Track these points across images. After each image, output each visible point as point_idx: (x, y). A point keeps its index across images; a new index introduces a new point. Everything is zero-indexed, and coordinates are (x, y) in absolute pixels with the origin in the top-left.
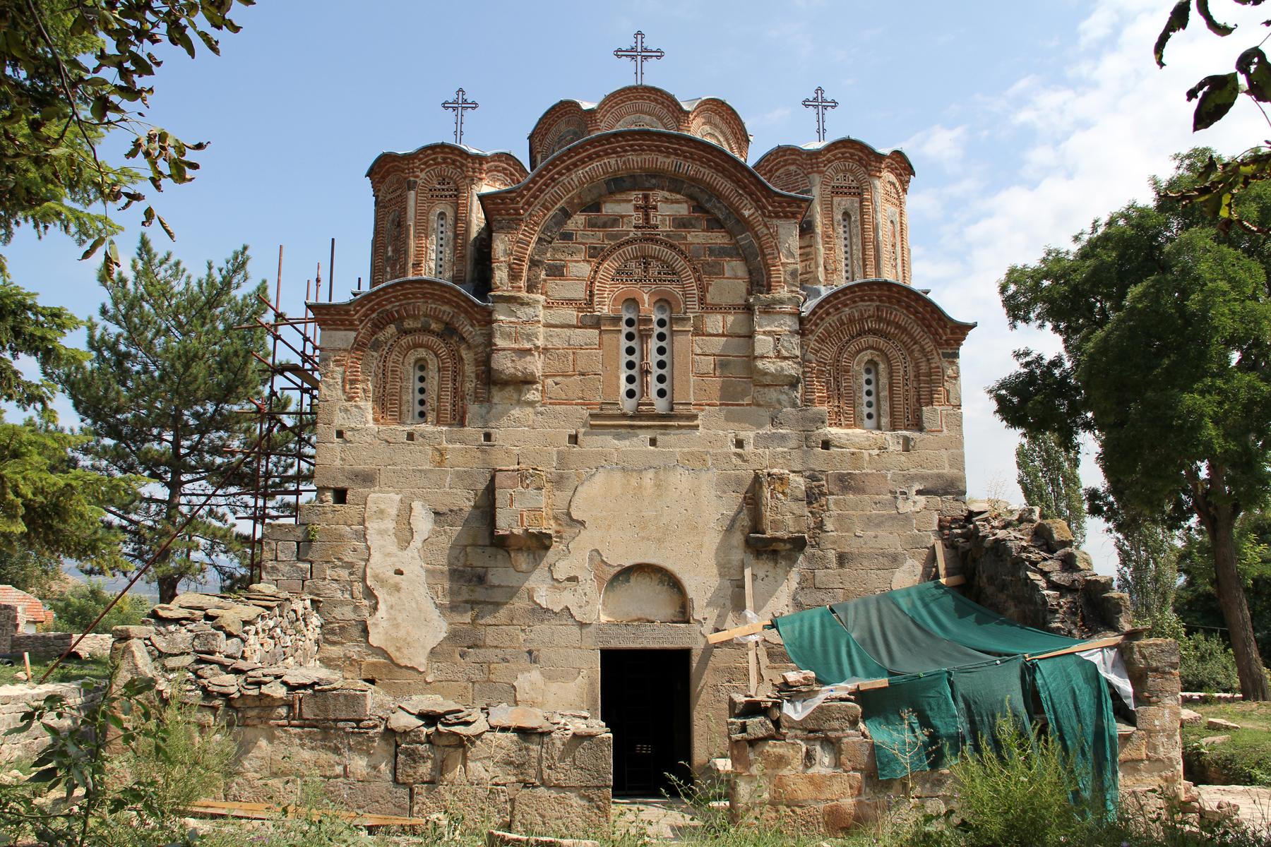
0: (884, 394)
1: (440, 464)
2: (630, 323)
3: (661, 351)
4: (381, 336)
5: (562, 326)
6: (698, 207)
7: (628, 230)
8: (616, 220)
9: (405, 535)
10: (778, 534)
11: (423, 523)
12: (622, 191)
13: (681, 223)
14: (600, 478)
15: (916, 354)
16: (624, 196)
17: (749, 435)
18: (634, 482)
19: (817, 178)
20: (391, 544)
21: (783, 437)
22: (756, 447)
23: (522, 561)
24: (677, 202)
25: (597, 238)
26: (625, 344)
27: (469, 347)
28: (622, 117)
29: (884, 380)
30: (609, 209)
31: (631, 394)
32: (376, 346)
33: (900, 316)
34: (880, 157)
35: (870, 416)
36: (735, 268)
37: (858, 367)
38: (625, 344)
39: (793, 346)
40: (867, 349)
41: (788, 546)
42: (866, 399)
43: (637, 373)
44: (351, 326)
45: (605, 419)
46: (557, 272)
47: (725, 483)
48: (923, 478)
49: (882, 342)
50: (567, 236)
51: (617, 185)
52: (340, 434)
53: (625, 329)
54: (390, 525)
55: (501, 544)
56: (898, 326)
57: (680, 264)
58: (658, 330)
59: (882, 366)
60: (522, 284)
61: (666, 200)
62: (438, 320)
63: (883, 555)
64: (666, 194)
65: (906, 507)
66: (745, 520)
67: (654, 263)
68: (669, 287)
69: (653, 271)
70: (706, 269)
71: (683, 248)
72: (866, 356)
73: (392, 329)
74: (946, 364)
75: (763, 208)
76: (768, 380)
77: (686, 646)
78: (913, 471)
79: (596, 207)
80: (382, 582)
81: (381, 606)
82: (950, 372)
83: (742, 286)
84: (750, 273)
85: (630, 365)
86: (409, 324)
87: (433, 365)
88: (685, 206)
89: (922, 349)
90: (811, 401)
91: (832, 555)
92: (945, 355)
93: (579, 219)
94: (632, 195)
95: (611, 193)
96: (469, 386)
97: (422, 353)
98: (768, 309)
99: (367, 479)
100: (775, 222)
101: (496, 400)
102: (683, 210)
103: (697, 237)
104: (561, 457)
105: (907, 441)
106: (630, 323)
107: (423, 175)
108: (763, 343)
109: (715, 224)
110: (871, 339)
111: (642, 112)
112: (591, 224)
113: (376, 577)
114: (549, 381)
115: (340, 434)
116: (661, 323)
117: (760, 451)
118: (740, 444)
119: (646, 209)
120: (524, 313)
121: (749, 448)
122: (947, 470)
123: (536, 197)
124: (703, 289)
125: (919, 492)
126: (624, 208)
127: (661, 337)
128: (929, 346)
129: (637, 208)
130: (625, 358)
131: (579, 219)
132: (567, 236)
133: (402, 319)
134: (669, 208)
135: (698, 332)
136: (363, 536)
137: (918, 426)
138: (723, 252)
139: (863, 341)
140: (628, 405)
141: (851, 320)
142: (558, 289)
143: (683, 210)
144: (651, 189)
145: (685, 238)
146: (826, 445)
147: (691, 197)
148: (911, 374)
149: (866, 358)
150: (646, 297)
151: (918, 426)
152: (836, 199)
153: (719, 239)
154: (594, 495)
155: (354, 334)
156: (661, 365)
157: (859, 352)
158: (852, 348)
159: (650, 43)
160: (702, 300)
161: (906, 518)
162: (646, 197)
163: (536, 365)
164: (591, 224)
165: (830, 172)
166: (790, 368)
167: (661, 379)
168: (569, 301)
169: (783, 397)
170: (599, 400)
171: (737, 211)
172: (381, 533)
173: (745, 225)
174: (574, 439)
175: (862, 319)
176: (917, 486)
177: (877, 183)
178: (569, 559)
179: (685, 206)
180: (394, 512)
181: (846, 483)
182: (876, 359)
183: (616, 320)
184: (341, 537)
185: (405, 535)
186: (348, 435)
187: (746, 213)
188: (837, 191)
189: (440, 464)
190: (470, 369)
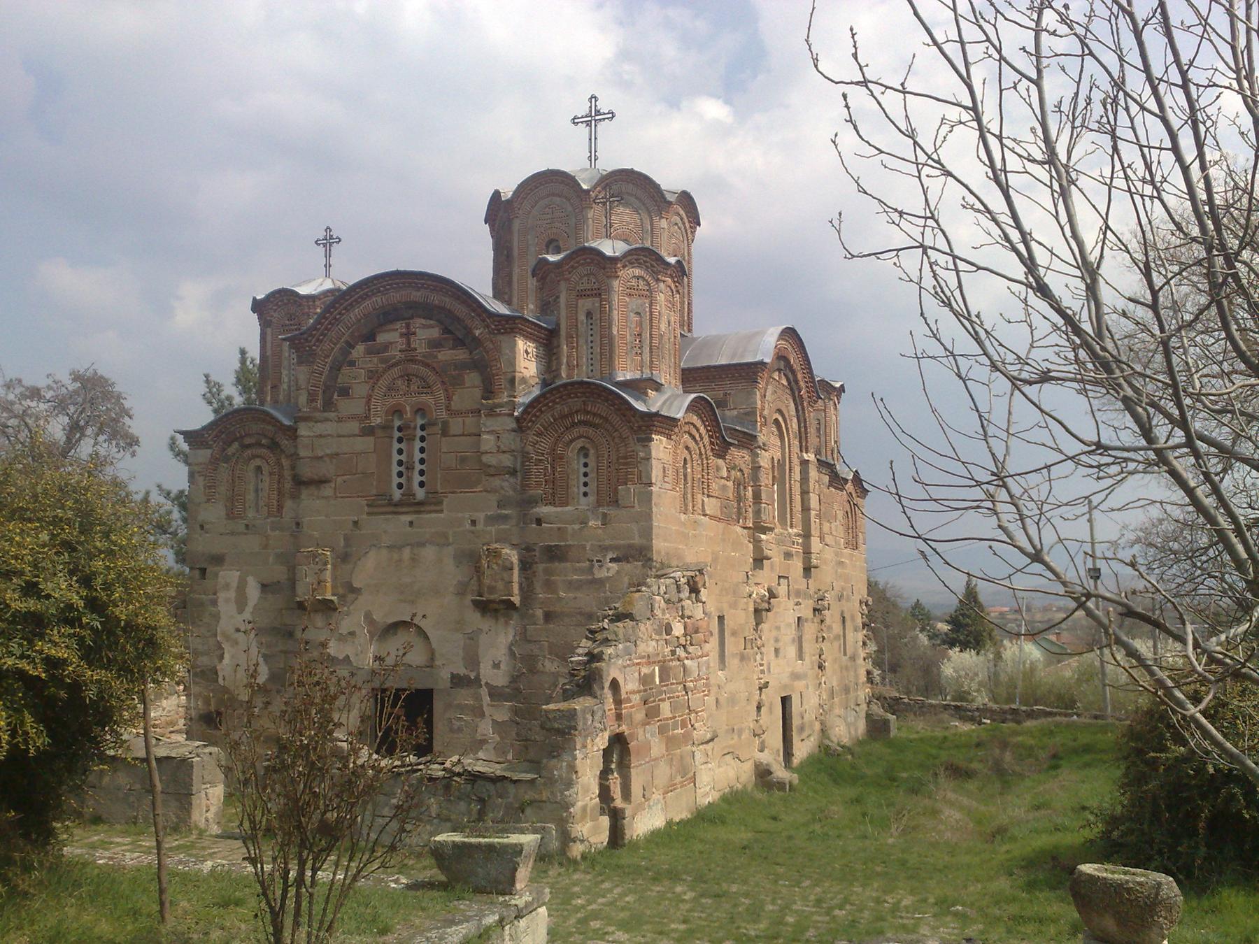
0: (594, 475)
1: (266, 547)
2: (400, 429)
3: (422, 450)
4: (231, 450)
5: (349, 436)
6: (446, 330)
7: (395, 353)
8: (386, 346)
9: (241, 603)
10: (492, 597)
11: (253, 592)
12: (391, 322)
13: (435, 344)
14: (372, 554)
15: (617, 440)
16: (391, 327)
17: (480, 516)
18: (396, 556)
19: (563, 285)
20: (232, 608)
21: (505, 518)
22: (486, 525)
23: (319, 620)
24: (431, 326)
25: (374, 362)
26: (396, 446)
27: (287, 457)
28: (536, 203)
29: (592, 464)
30: (382, 338)
31: (400, 486)
32: (227, 459)
33: (602, 408)
34: (614, 260)
35: (585, 494)
36: (472, 378)
37: (571, 453)
38: (396, 446)
39: (510, 441)
40: (579, 438)
41: (502, 606)
42: (583, 479)
43: (406, 467)
44: (210, 447)
45: (384, 505)
46: (345, 392)
47: (460, 557)
48: (616, 548)
49: (591, 431)
50: (352, 364)
51: (388, 317)
52: (202, 527)
53: (397, 434)
54: (232, 594)
55: (301, 606)
56: (601, 417)
57: (432, 378)
58: (419, 433)
59: (592, 452)
60: (319, 404)
61: (424, 327)
62: (265, 436)
63: (581, 614)
64: (423, 321)
65: (600, 574)
66: (474, 585)
67: (414, 379)
68: (425, 398)
69: (414, 387)
70: (451, 379)
71: (435, 365)
72: (579, 444)
73: (236, 445)
74: (639, 448)
75: (488, 326)
76: (492, 471)
77: (429, 686)
78: (607, 543)
79: (371, 337)
80: (227, 638)
81: (227, 656)
82: (642, 455)
83: (477, 393)
84: (483, 381)
85: (400, 463)
86: (247, 441)
87: (266, 469)
88: (437, 329)
89: (621, 437)
90: (527, 486)
91: (539, 613)
92: (639, 440)
93: (360, 348)
94: (398, 325)
95: (381, 325)
96: (288, 485)
97: (258, 462)
98: (491, 412)
99: (218, 560)
100: (501, 337)
101: (303, 497)
102: (435, 333)
103: (445, 355)
104: (347, 539)
105: (605, 515)
106: (400, 429)
107: (276, 315)
108: (488, 441)
109: (459, 343)
110: (583, 430)
111: (554, 195)
112: (369, 352)
113: (223, 634)
114: (339, 480)
115: (202, 527)
116: (423, 428)
117: (489, 528)
118: (474, 523)
119: (408, 335)
120: (320, 428)
121: (480, 527)
122: (637, 541)
123: (325, 335)
124: (449, 399)
125: (612, 560)
126: (391, 336)
127: (423, 439)
128: (626, 432)
129: (402, 335)
130: (396, 457)
131: (360, 348)
132: (352, 364)
133: (242, 437)
134: (425, 332)
135: (445, 433)
136: (214, 603)
137: (615, 502)
138: (463, 366)
139: (576, 431)
140: (397, 495)
141: (564, 417)
142: (348, 407)
143: (435, 333)
144: (412, 317)
145: (436, 357)
146: (539, 522)
147: (440, 322)
148: (614, 458)
149: (579, 446)
150: (408, 408)
151: (615, 502)
152: (581, 302)
153: (461, 355)
154: (367, 569)
155: (209, 451)
156: (422, 461)
157: (572, 441)
158: (567, 437)
159: (603, 106)
160: (448, 409)
161: (601, 582)
162: (408, 326)
163: (327, 469)
164: (369, 352)
165: (575, 278)
166: (507, 460)
167: (422, 473)
168: (353, 417)
169: (506, 484)
170: (374, 492)
171: (469, 331)
172: (227, 601)
173: (477, 342)
174: (356, 523)
175: (571, 414)
176: (610, 555)
177: (616, 283)
178: (352, 620)
179: (437, 329)
180: (234, 584)
181: (555, 554)
182: (587, 446)
183: (386, 427)
184: (202, 604)
185: (241, 603)
186: (206, 527)
187: (477, 333)
188: (582, 295)
189: (266, 547)
190: (287, 474)
